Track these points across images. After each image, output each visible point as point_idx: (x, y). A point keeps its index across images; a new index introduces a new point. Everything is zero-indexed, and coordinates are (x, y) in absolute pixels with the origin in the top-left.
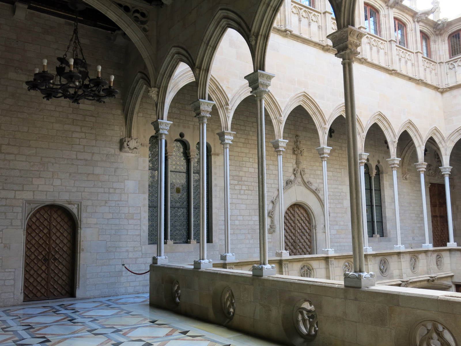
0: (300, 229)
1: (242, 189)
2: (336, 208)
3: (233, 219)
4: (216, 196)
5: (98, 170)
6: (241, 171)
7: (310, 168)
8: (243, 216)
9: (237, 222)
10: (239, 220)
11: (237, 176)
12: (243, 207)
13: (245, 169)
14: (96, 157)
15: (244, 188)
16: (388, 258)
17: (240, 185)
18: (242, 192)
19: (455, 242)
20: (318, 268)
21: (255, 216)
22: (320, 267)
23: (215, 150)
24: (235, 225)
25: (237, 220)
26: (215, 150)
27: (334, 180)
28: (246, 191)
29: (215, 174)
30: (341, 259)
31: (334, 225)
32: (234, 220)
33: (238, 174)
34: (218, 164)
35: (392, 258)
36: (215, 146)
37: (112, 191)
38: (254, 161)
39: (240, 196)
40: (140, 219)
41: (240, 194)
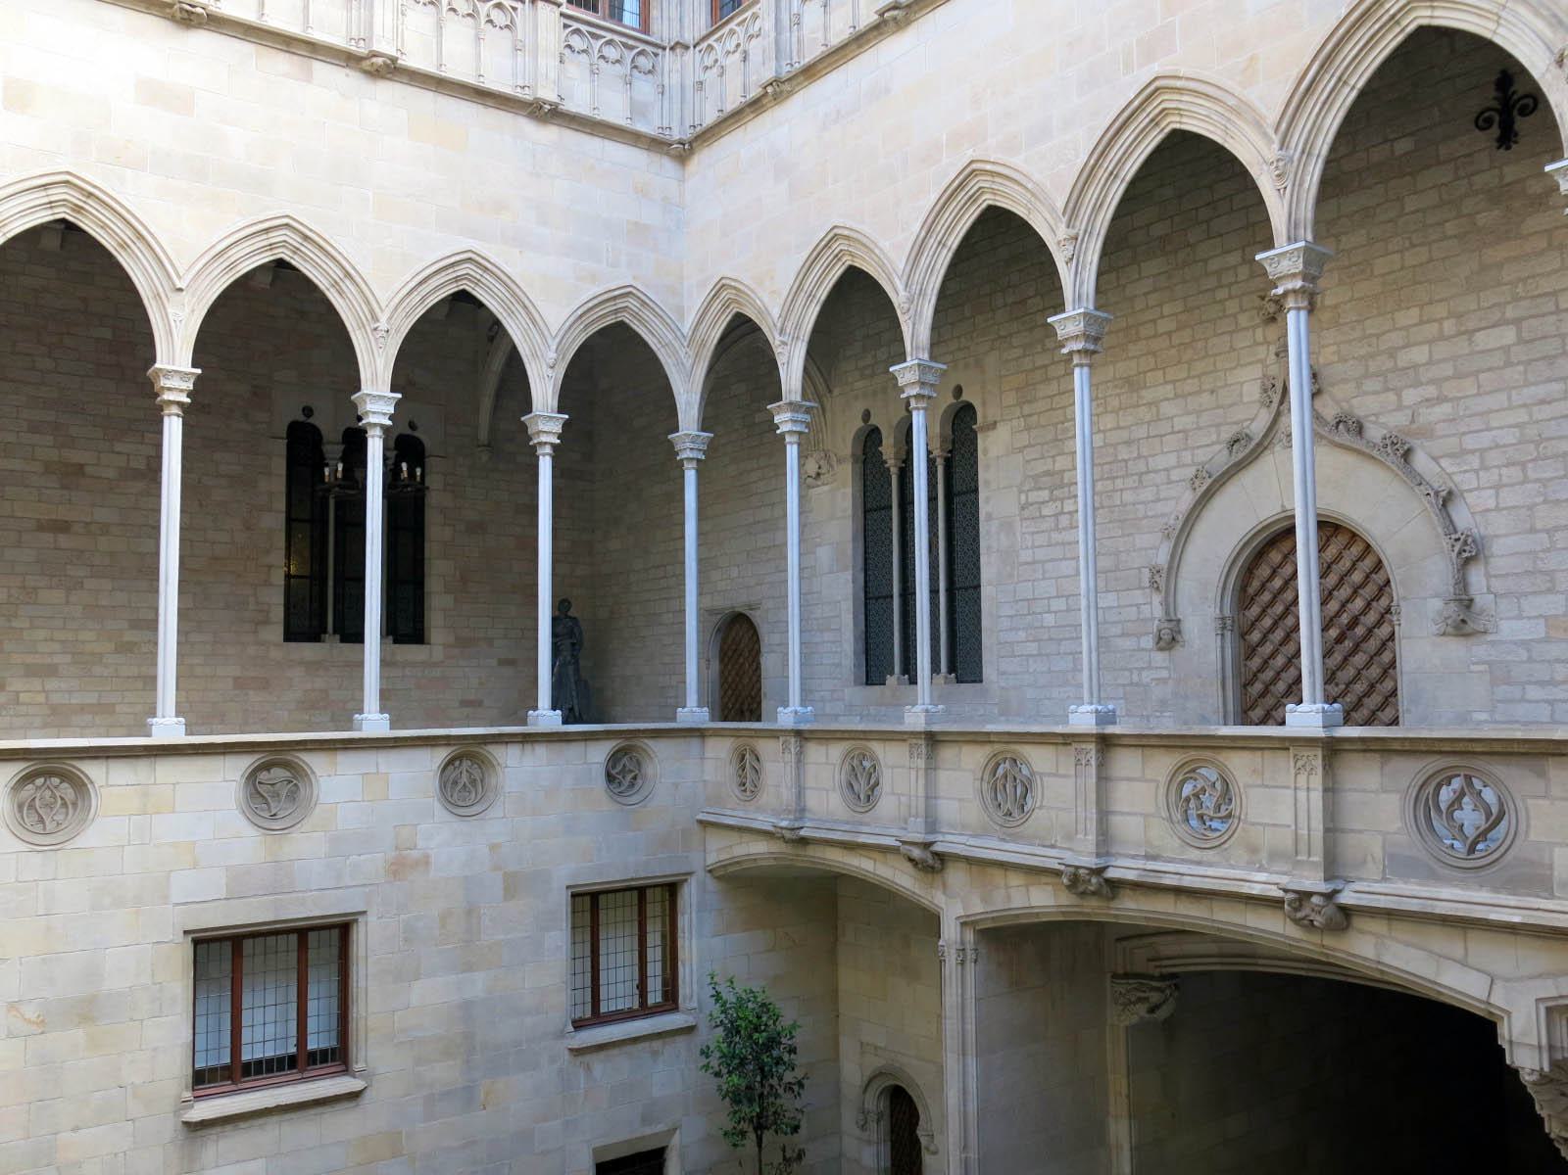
1: (1062, 513)
2: (1545, 502)
3: (1038, 610)
4: (989, 548)
6: (1059, 454)
7: (1362, 352)
8: (1068, 597)
9: (1049, 620)
10: (1055, 612)
11: (1048, 473)
17: (1055, 501)
20: (1050, 775)
21: (1108, 591)
22: (1062, 771)
23: (985, 417)
24: (1042, 627)
25: (1049, 612)
26: (985, 417)
27: (1529, 362)
29: (987, 483)
30: (1162, 750)
31: (1526, 595)
32: (1040, 613)
33: (1051, 467)
34: (994, 452)
35: (1542, 774)
36: (984, 404)
38: (1101, 409)
39: (1056, 537)
40: (839, 630)
41: (1057, 529)
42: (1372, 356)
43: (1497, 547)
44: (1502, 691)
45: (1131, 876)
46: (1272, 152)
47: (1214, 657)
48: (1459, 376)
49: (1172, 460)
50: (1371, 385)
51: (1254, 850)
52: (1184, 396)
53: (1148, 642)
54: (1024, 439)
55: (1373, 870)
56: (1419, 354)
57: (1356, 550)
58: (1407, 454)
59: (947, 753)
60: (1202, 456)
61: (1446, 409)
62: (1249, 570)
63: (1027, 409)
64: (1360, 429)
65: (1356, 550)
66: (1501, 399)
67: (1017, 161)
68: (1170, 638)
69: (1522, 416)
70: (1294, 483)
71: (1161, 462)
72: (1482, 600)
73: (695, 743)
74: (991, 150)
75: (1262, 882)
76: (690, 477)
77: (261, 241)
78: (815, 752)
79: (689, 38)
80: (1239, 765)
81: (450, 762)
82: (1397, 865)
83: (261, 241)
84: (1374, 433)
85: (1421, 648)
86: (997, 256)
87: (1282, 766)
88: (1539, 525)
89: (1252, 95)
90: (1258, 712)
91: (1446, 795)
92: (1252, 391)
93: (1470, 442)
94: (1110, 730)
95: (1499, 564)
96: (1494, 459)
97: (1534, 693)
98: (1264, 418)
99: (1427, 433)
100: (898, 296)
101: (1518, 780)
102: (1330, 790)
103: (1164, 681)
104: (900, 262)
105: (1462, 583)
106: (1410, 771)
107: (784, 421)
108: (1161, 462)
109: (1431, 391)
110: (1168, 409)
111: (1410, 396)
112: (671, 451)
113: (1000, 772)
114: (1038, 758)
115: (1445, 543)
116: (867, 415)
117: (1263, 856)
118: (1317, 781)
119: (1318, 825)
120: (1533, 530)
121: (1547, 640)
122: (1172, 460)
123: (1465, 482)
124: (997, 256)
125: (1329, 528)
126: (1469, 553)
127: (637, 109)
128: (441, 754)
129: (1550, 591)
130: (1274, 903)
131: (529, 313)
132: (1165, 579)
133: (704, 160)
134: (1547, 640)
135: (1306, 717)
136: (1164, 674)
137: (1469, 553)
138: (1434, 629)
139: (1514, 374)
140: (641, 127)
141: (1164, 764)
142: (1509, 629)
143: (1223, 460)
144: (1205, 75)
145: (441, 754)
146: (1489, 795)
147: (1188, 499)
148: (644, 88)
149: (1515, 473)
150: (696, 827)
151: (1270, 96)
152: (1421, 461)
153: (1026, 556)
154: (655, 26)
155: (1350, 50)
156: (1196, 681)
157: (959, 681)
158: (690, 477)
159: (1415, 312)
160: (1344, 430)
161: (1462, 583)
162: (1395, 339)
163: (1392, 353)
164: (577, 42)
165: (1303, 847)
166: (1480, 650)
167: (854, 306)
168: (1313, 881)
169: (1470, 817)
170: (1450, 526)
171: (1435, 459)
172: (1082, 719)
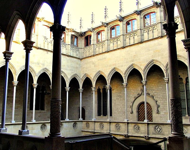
0: (143, 112)
4: (113, 102)
5: (88, 99)
9: (120, 110)
11: (119, 95)
12: (121, 105)
13: (122, 93)
14: (88, 96)
15: (122, 99)
16: (90, 123)
18: (121, 100)
19: (82, 118)
23: (113, 89)
26: (113, 89)
28: (123, 100)
34: (114, 93)
37: (90, 104)
41: (120, 101)
42: (150, 88)
43: (160, 106)
44: (161, 119)
45: (130, 135)
46: (143, 72)
47: (136, 115)
48: (157, 90)
49: (132, 95)
50: (150, 90)
51: (141, 132)
52: (133, 89)
53: (130, 113)
54: (117, 92)
55: (151, 134)
56: (154, 88)
57: (149, 105)
58: (153, 97)
59: (111, 124)
60: (135, 95)
61: (156, 93)
62: (139, 107)
63: (117, 89)
64: (149, 94)
65: (149, 105)
66: (160, 93)
67: (120, 68)
68: (132, 113)
69: (162, 95)
70: (144, 98)
71: (131, 95)
72: (159, 110)
73: (81, 122)
74: (117, 66)
75: (142, 135)
76: (81, 94)
77: (43, 71)
78: (96, 123)
79: (82, 48)
80: (140, 125)
81: (42, 125)
82: (153, 134)
83: (43, 71)
84: (151, 95)
85: (154, 115)
86: (117, 76)
87: (144, 125)
88: (164, 104)
89: (141, 67)
90: (140, 120)
91: (157, 128)
92: (140, 90)
93: (158, 97)
94: (128, 122)
95: (161, 107)
96: (160, 98)
97: (164, 119)
98: (141, 92)
99: (155, 95)
100: (107, 79)
101: (162, 126)
102: (148, 127)
103: (131, 117)
104: (107, 75)
105: (158, 109)
106: (154, 126)
107: (93, 89)
108: (131, 95)
109: (155, 92)
110: (132, 90)
111: (154, 92)
112: (79, 91)
113: (117, 126)
114: (121, 124)
115: (156, 105)
116: (99, 87)
117: (142, 133)
118: (147, 127)
119: (147, 130)
120: (163, 105)
121: (165, 114)
122: (132, 95)
123: (158, 100)
124: (117, 76)
125: (147, 103)
126: (158, 107)
127: (77, 55)
128: (41, 124)
129: (165, 110)
130: (143, 137)
131: (67, 77)
132: (132, 107)
133: (82, 60)
134: (165, 114)
135: (146, 121)
136: (131, 116)
137: (158, 107)
138: (155, 113)
139: (162, 91)
140: (77, 57)
141: (133, 125)
142: (162, 113)
143: (137, 96)
144: (137, 65)
145: (41, 124)
146: (160, 128)
147: (134, 99)
148: (78, 52)
149: (162, 100)
150: (81, 131)
151: (143, 68)
152: (154, 98)
153: (117, 104)
154: (79, 46)
155: (149, 65)
156: (134, 118)
157: (104, 116)
158: (81, 94)
159: (154, 84)
160: (148, 94)
161: (158, 109)
162: (152, 86)
163: (152, 88)
164: (72, 48)
165: (146, 132)
166: (159, 115)
167: (101, 79)
168: (147, 135)
169: (159, 130)
170: (157, 104)
171: (156, 98)
172: (126, 121)
